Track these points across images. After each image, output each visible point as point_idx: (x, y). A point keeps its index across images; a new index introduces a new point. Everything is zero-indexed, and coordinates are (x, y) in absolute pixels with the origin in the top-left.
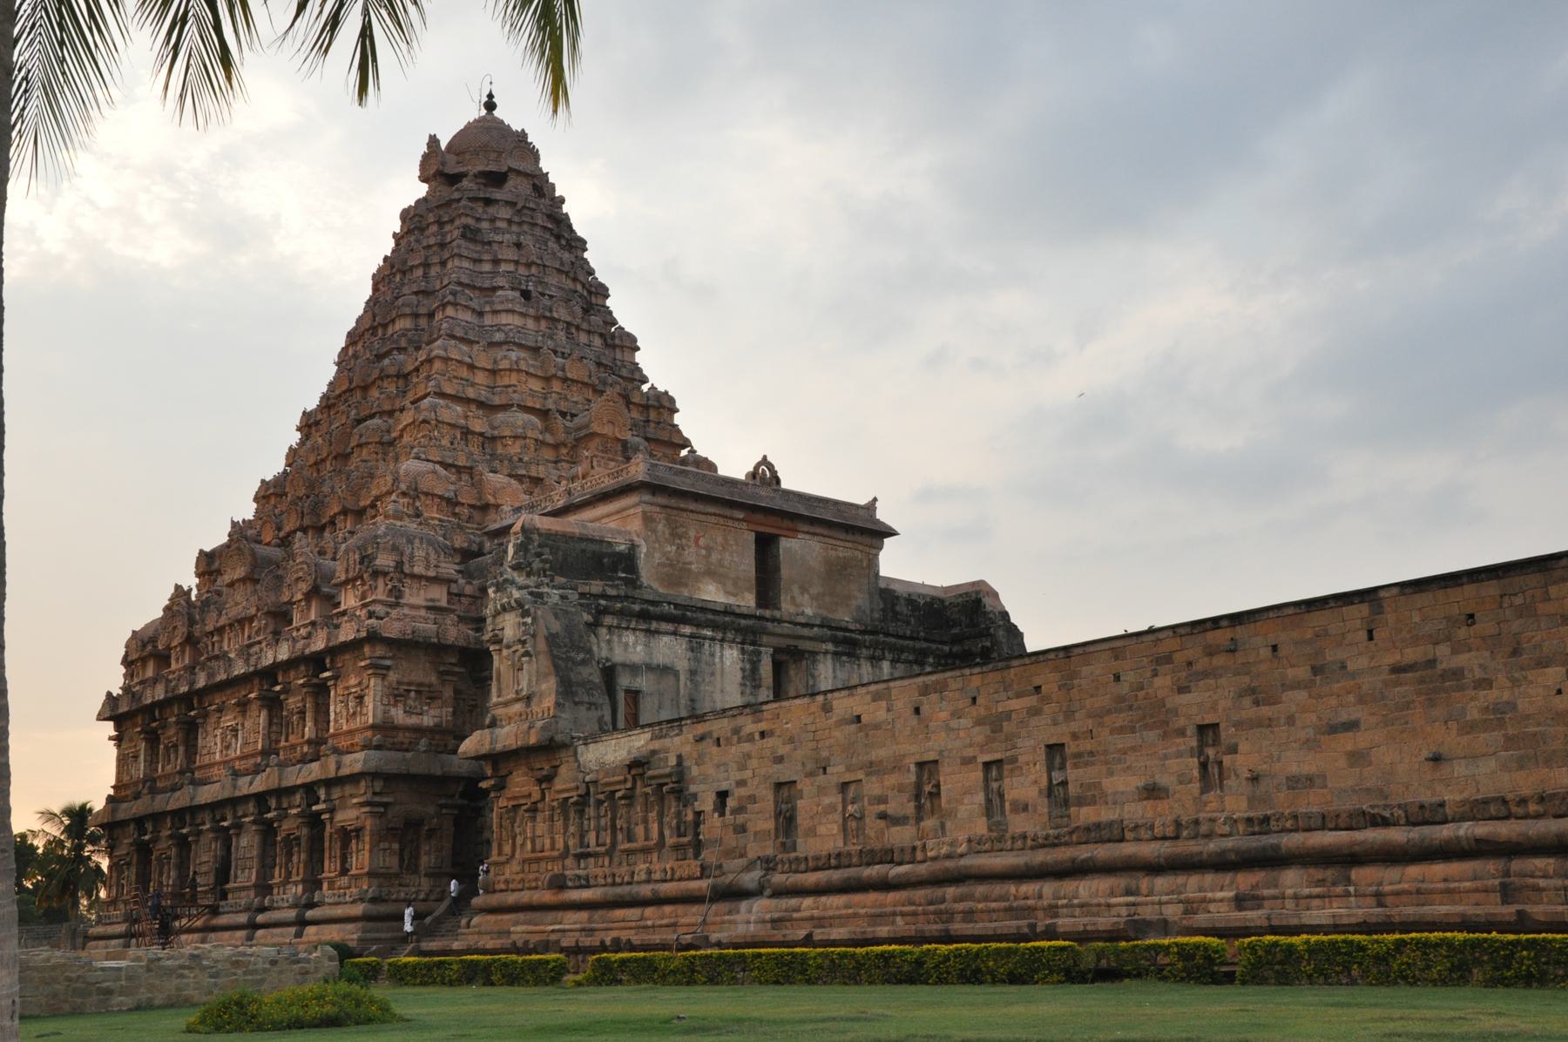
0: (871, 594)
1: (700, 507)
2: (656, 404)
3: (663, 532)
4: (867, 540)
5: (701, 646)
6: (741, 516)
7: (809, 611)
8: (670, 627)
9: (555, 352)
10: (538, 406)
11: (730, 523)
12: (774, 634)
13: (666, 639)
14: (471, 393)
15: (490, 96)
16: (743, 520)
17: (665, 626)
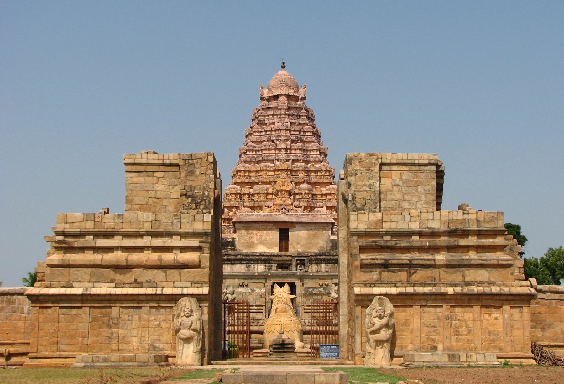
0: (327, 242)
1: (256, 225)
2: (320, 169)
3: (244, 234)
4: (325, 225)
5: (250, 266)
6: (272, 225)
7: (300, 250)
8: (238, 262)
9: (278, 160)
10: (268, 181)
11: (269, 227)
12: (275, 260)
13: (238, 265)
14: (247, 181)
15: (283, 63)
16: (273, 226)
17: (236, 262)
